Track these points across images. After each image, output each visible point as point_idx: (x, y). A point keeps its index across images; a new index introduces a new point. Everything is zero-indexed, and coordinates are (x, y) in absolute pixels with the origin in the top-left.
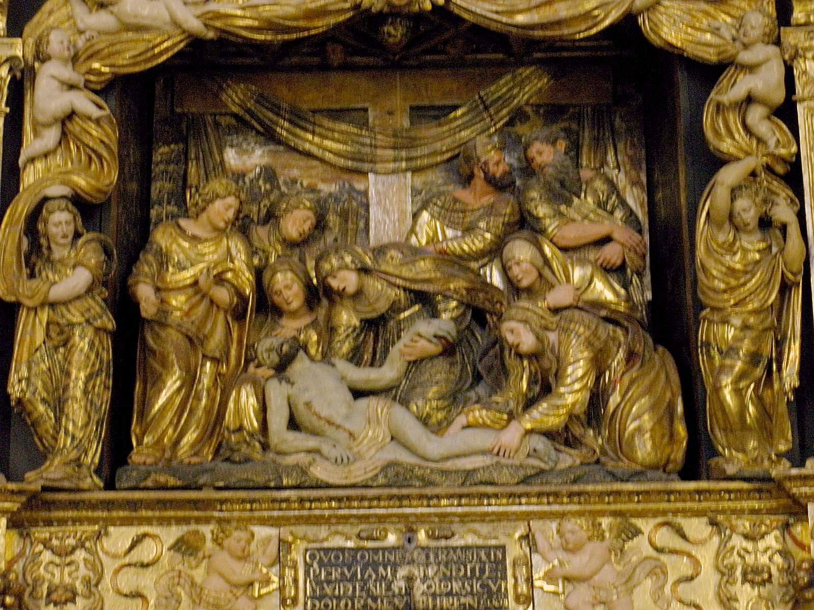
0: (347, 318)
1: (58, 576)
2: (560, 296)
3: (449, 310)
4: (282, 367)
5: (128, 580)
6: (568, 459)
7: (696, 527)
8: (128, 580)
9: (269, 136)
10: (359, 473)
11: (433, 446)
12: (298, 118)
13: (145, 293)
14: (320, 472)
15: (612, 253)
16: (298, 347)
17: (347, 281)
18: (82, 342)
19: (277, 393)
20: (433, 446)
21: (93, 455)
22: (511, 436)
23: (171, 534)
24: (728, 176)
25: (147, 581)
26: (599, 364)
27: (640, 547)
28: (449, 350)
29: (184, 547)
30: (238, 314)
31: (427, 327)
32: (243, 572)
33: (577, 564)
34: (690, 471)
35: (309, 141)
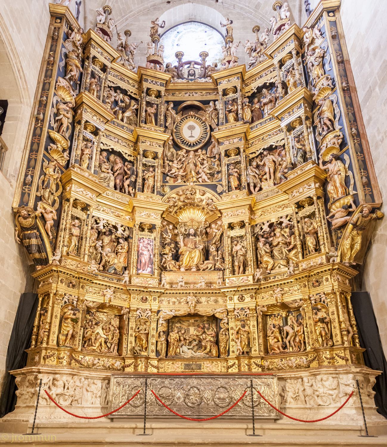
0: (188, 341)
1: (162, 366)
2: (207, 340)
3: (197, 341)
4: (182, 346)
5: (168, 366)
6: (207, 356)
7: (219, 362)
8: (168, 366)
9: (180, 323)
10: (188, 357)
11: (195, 354)
12: (183, 321)
13: (169, 340)
14: (185, 357)
15: (212, 335)
16: (183, 344)
17: (188, 338)
18: (164, 345)
19: (181, 349)
20: (195, 354)
21: (165, 355)
22: (202, 354)
23: (171, 362)
24: (222, 330)
25: (169, 366)
26: (211, 347)
27: (213, 364)
28: (197, 345)
29: (173, 363)
30: (177, 341)
31: (195, 343)
32: (178, 366)
33: (208, 365)
34: (219, 357)
35: (184, 323)
